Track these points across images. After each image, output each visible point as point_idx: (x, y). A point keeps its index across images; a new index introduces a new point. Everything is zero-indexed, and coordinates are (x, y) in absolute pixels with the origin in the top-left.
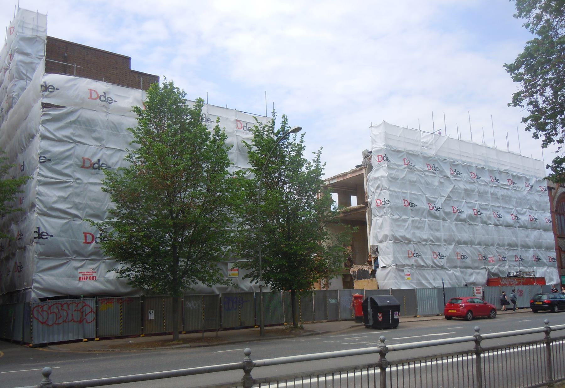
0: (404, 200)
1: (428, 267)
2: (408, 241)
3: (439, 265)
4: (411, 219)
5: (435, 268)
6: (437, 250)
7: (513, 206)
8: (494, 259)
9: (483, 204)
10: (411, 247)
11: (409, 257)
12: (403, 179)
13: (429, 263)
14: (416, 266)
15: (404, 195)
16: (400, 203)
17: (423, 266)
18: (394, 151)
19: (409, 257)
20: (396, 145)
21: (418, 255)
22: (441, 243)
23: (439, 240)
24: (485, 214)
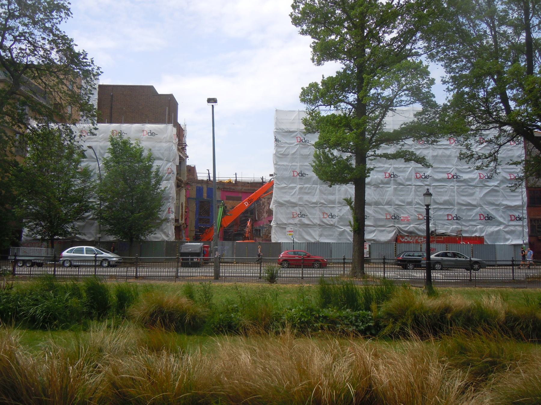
0: (293, 171)
1: (315, 225)
2: (294, 205)
3: (329, 223)
4: (299, 186)
5: (323, 226)
6: (328, 211)
7: (453, 165)
8: (409, 218)
9: (401, 168)
10: (297, 210)
11: (293, 217)
12: (293, 154)
13: (317, 221)
14: (299, 224)
15: (294, 167)
16: (288, 174)
17: (308, 225)
18: (286, 132)
19: (293, 217)
20: (286, 127)
21: (303, 215)
22: (335, 205)
23: (333, 202)
24: (402, 176)
